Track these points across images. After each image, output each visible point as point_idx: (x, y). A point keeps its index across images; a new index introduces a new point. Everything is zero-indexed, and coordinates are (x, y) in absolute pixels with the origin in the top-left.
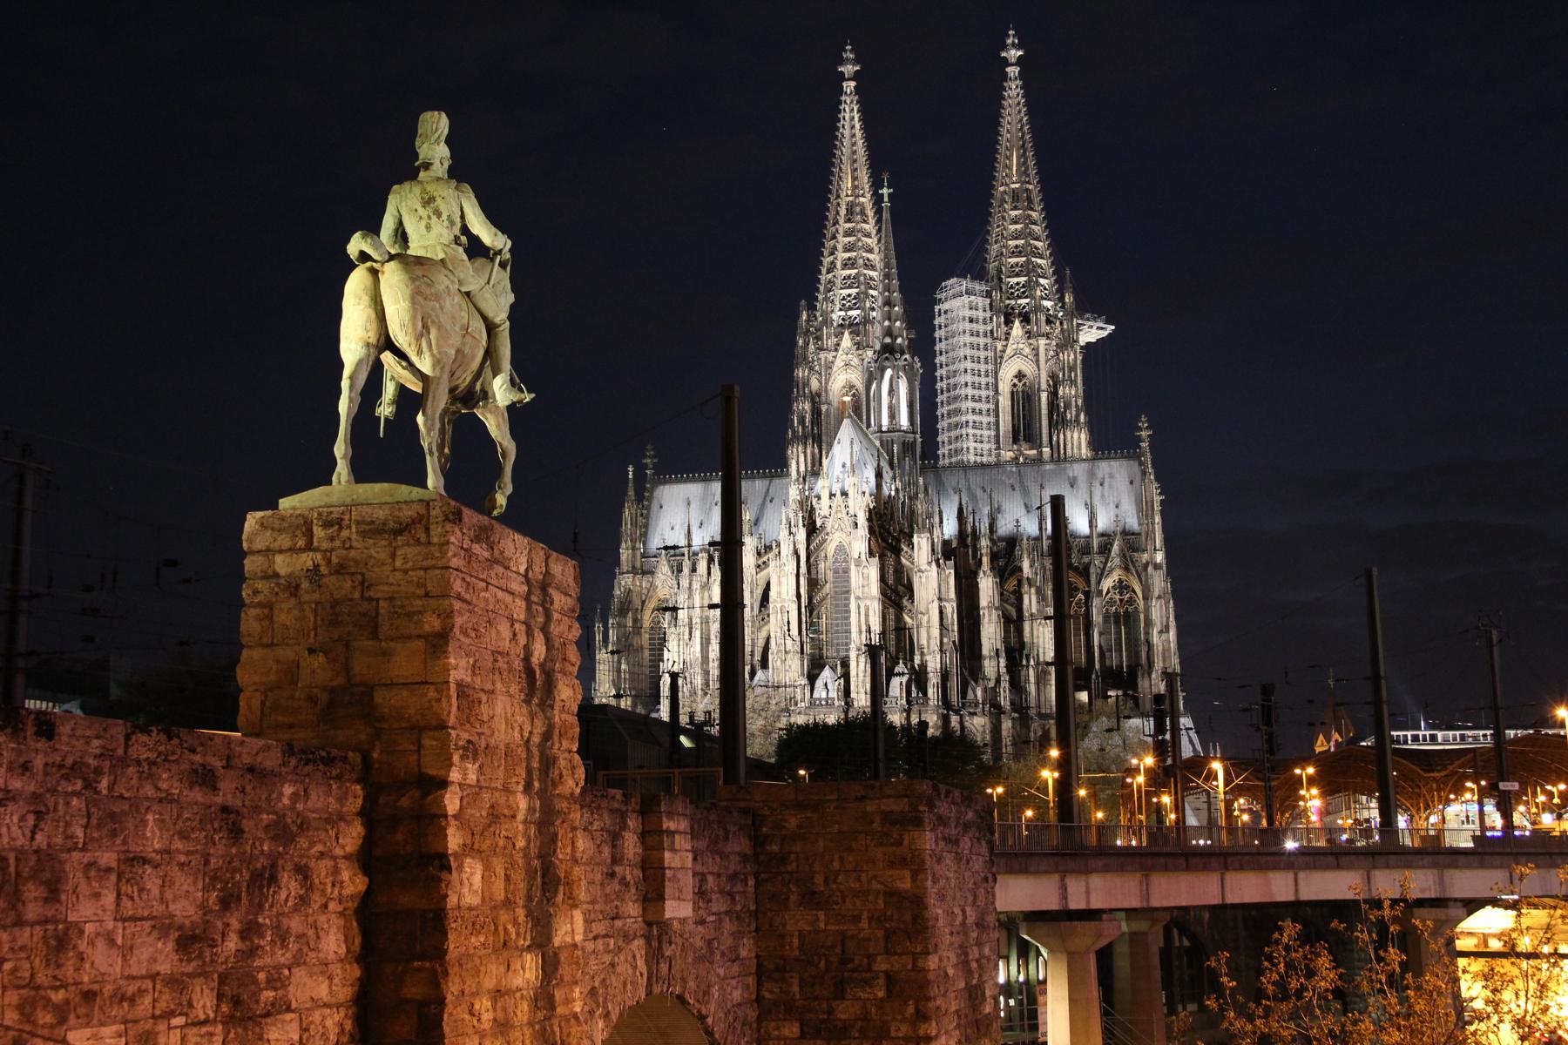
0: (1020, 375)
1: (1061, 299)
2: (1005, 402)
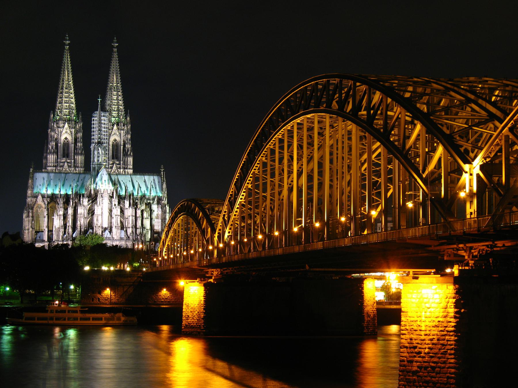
0: (115, 140)
1: (126, 118)
2: (111, 147)
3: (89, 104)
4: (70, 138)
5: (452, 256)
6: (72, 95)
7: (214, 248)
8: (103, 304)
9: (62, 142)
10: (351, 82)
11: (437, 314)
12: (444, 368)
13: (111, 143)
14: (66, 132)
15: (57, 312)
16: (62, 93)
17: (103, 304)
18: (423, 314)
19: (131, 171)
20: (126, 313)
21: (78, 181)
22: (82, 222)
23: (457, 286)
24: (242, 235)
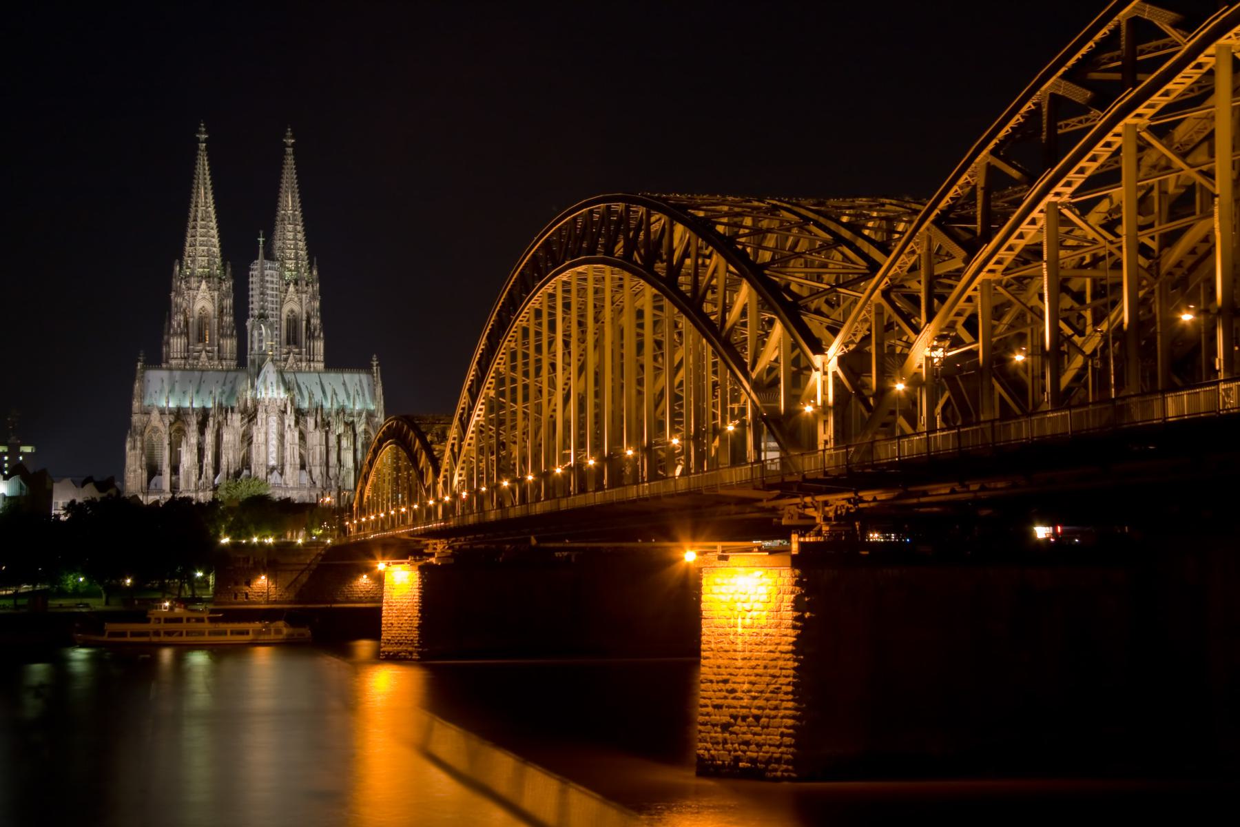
1: (311, 272)
2: (284, 324)
3: (243, 245)
4: (210, 308)
5: (796, 517)
6: (214, 232)
7: (437, 501)
8: (255, 603)
9: (196, 315)
10: (642, 210)
11: (763, 622)
12: (775, 717)
13: (284, 317)
14: (204, 298)
15: (167, 620)
16: (194, 228)
17: (255, 603)
18: (739, 621)
19: (321, 366)
20: (291, 618)
21: (224, 384)
22: (230, 457)
23: (797, 572)
24: (480, 480)
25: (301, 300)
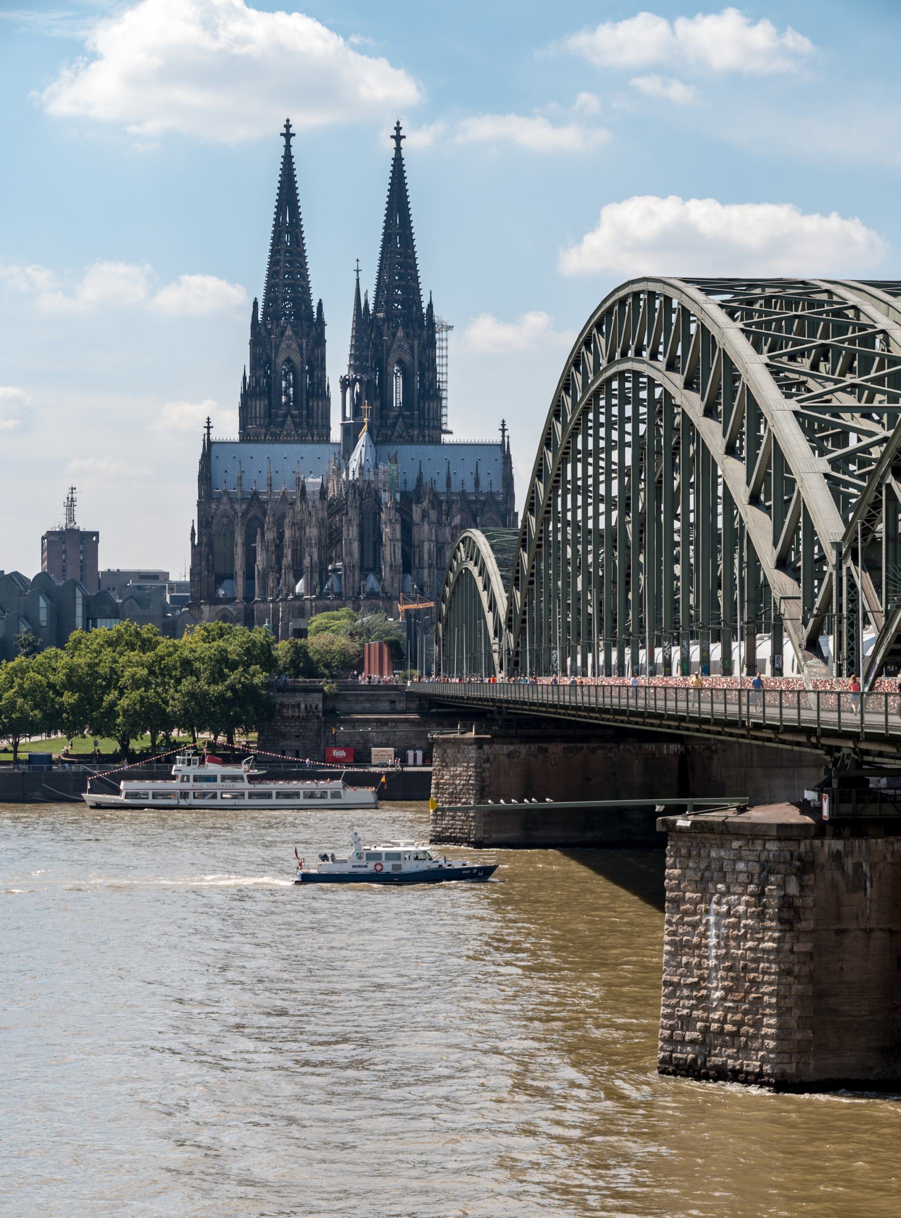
25: (412, 348)
